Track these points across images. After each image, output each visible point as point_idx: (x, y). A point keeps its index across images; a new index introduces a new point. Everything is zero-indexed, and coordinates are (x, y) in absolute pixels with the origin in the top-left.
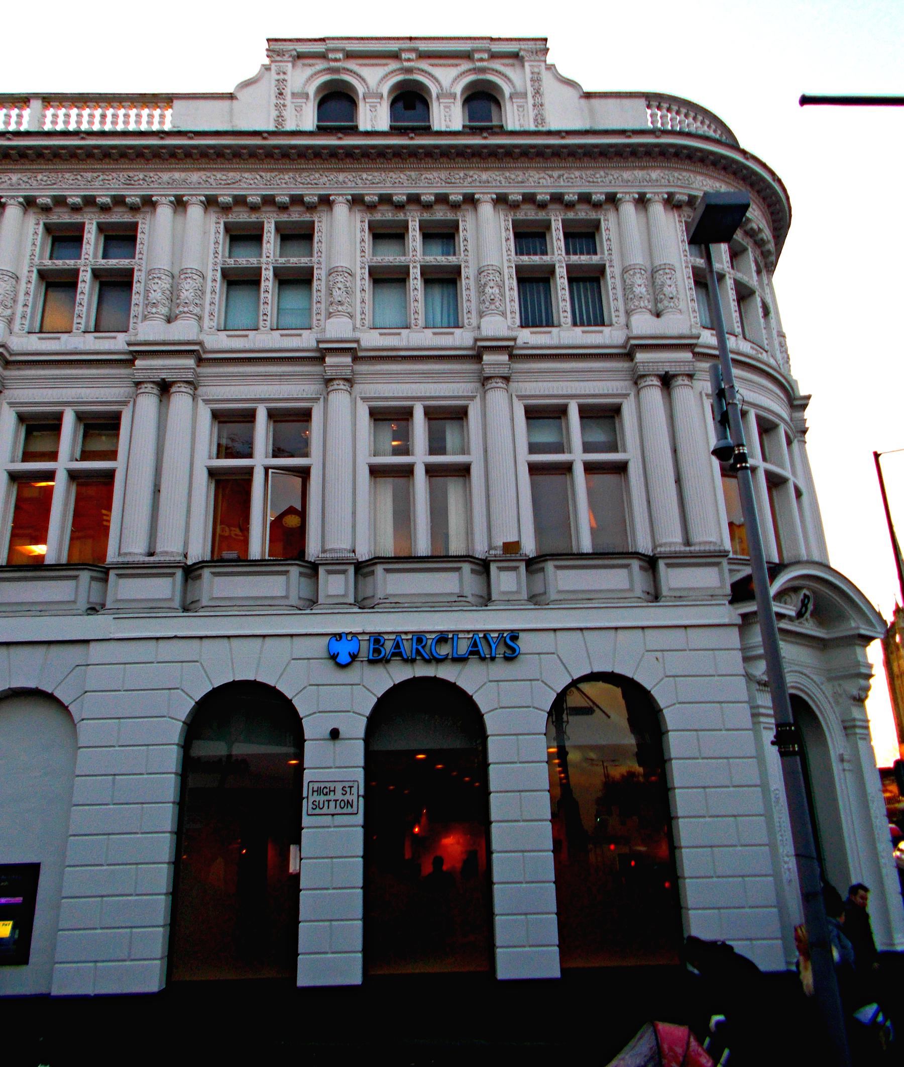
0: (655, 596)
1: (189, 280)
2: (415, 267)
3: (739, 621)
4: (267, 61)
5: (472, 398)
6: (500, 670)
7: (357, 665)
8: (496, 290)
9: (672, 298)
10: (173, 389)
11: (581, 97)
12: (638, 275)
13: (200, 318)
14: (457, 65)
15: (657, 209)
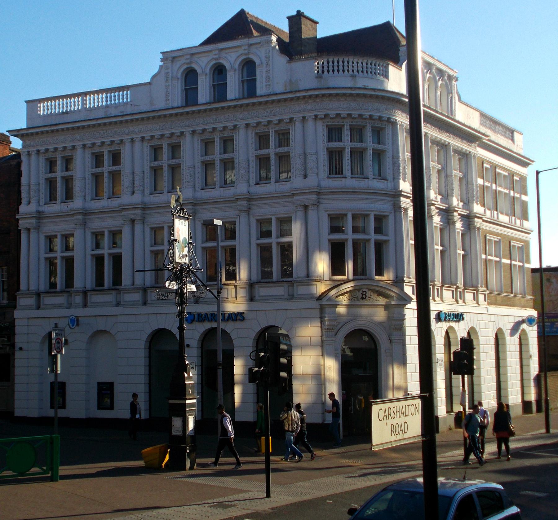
0: (292, 297)
1: (137, 176)
2: (217, 160)
3: (319, 307)
4: (162, 63)
5: (237, 218)
6: (238, 324)
7: (194, 322)
8: (244, 171)
9: (311, 169)
10: (135, 222)
11: (286, 63)
12: (298, 159)
13: (144, 190)
14: (237, 51)
15: (310, 124)
